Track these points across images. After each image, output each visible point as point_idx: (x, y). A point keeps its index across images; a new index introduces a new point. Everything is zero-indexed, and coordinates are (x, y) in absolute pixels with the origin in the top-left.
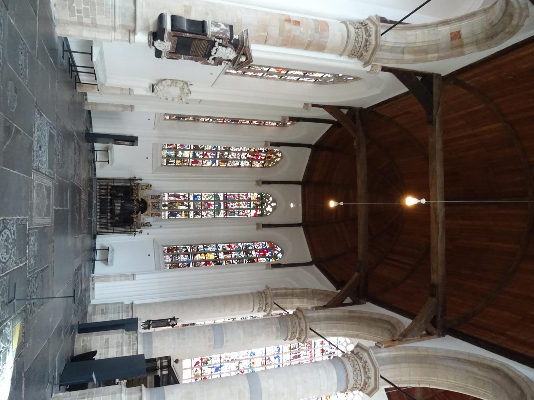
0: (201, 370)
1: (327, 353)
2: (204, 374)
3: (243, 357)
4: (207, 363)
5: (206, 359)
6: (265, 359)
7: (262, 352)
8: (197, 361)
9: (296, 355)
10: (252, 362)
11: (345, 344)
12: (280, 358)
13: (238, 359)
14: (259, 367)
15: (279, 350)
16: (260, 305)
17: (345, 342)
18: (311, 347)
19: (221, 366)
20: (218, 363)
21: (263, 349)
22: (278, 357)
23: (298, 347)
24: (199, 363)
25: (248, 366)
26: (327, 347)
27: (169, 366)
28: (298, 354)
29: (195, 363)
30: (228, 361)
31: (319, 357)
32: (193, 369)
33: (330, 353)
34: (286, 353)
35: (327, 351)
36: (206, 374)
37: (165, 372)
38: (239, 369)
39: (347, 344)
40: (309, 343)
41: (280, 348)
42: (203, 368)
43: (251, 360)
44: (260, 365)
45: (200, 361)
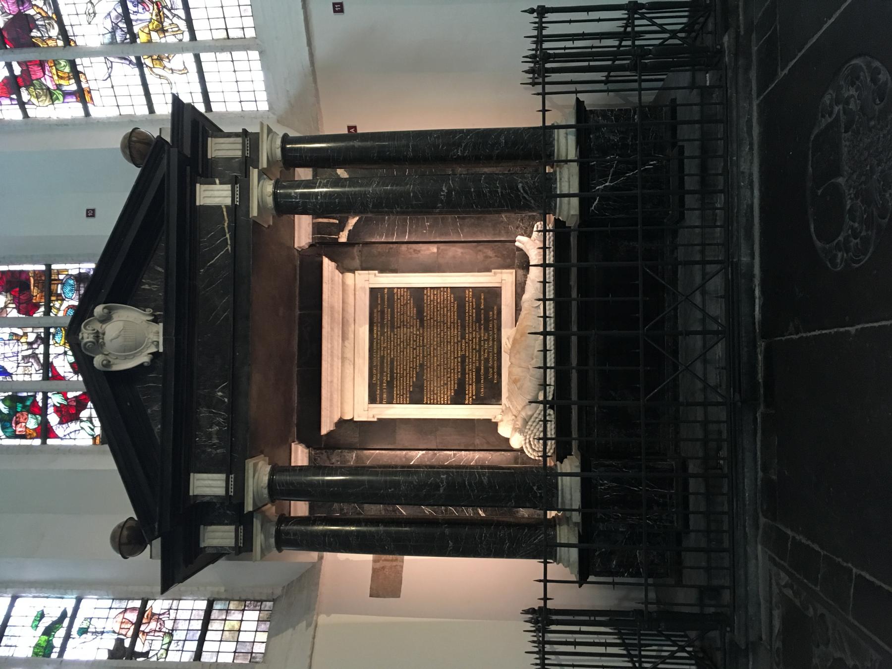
2: (32, 337)
4: (13, 400)
5: (19, 429)
8: (74, 426)
24: (58, 410)
36: (19, 332)
42: (37, 377)
45: (53, 419)
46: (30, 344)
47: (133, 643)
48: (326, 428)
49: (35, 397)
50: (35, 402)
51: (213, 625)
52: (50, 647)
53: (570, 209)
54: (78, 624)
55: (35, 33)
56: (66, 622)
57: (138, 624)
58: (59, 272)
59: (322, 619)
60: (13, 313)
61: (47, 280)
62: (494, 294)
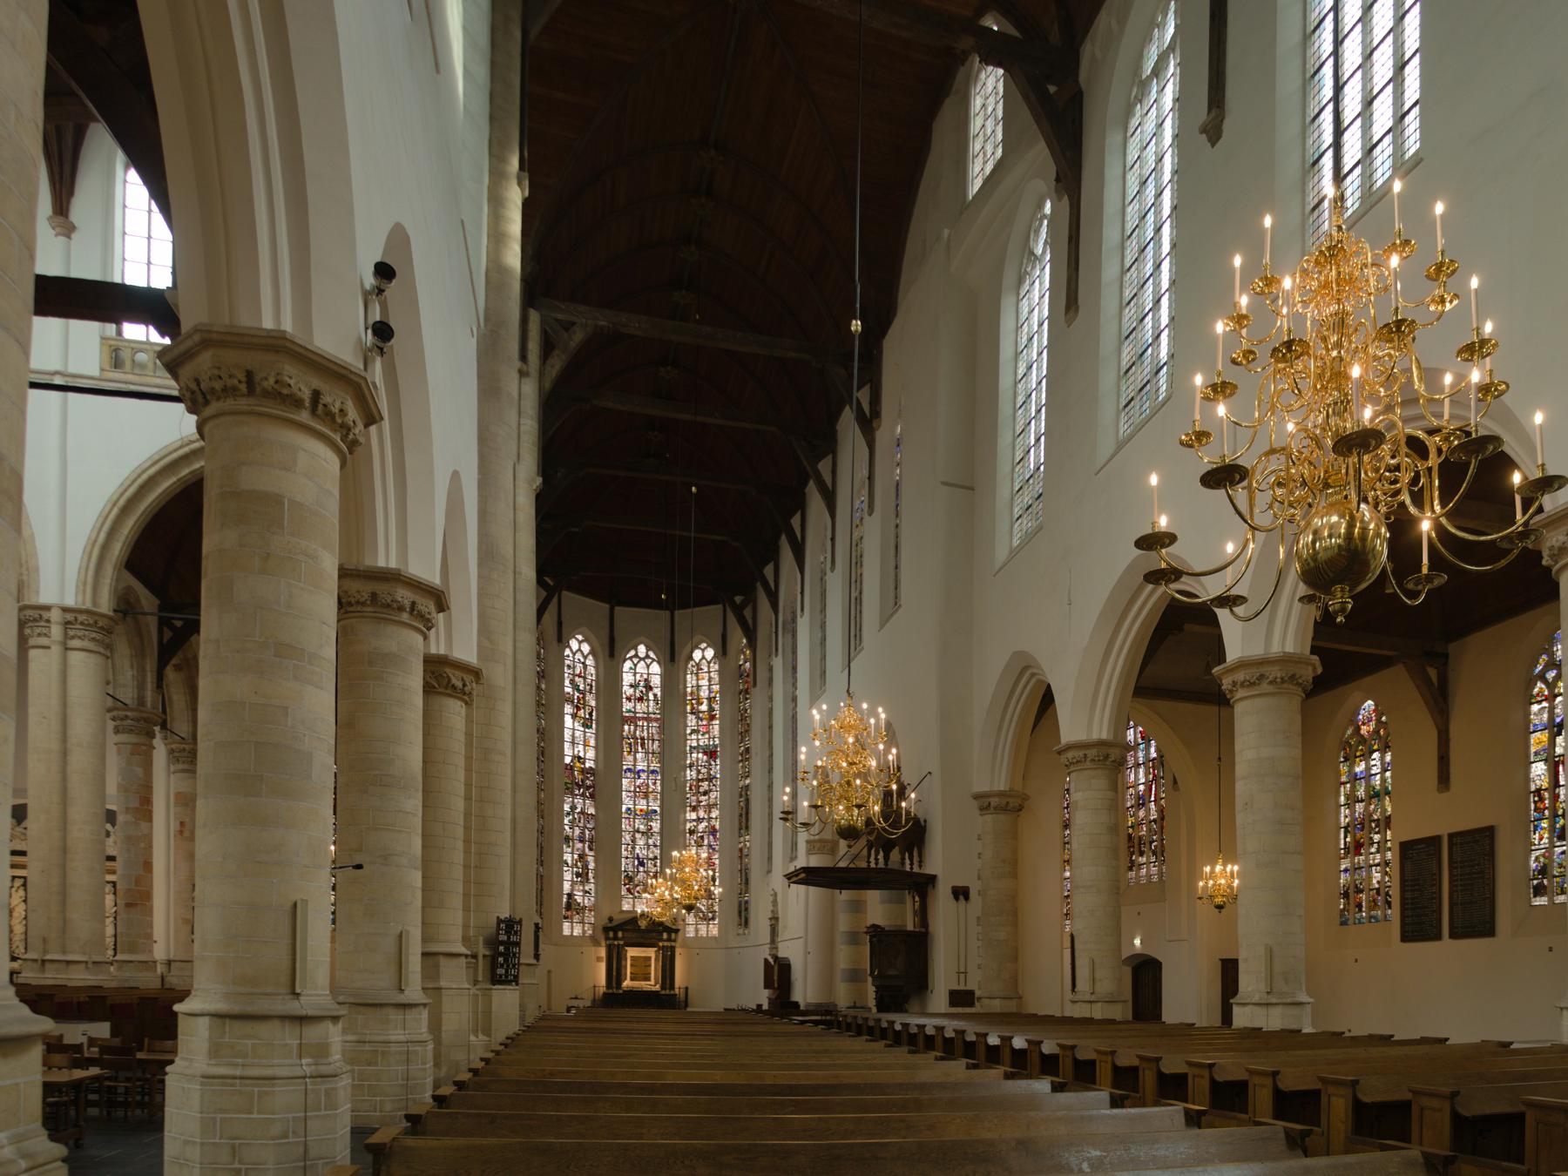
7: (628, 796)
11: (635, 660)
14: (648, 803)
15: (629, 770)
17: (634, 659)
18: (632, 717)
21: (624, 793)
22: (639, 771)
23: (629, 739)
26: (635, 692)
27: (615, 929)
31: (648, 707)
34: (635, 759)
35: (642, 692)
39: (636, 656)
40: (627, 721)
44: (644, 802)
48: (626, 948)
53: (663, 992)
59: (593, 948)
62: (649, 980)
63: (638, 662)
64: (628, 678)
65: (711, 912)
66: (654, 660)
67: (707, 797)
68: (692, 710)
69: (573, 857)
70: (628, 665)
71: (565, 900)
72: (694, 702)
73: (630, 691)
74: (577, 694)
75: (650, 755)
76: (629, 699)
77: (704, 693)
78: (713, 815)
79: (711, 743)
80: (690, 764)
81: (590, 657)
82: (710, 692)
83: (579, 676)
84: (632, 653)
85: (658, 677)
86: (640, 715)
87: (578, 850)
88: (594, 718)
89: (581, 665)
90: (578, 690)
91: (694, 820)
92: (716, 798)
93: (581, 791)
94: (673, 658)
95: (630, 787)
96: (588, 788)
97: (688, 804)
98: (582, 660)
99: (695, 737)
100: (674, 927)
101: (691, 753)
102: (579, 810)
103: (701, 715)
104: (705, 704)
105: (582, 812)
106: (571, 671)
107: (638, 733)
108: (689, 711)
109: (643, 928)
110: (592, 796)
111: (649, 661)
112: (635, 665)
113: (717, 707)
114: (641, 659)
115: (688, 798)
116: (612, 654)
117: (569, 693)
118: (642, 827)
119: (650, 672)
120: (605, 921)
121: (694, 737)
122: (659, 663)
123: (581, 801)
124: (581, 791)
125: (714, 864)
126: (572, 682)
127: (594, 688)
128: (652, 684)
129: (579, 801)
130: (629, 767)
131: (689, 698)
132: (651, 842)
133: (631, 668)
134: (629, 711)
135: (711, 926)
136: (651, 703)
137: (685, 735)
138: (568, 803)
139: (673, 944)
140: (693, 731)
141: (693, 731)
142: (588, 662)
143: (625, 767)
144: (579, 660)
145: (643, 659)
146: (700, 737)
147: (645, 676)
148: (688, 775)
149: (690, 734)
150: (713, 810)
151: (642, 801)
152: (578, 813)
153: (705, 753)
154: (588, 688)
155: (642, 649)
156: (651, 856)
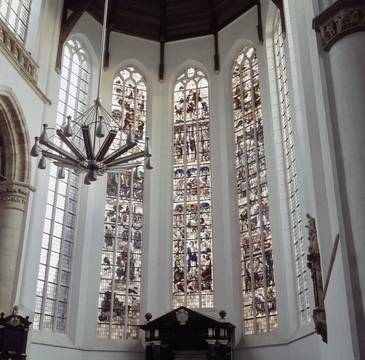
0: (190, 281)
1: (194, 103)
2: (196, 277)
3: (181, 222)
6: (189, 189)
7: (179, 195)
8: (177, 288)
9: (189, 147)
10: (189, 208)
12: (191, 169)
13: (182, 229)
15: (180, 171)
16: (9, 200)
17: (184, 81)
18: (182, 126)
19: (189, 252)
20: (184, 258)
21: (175, 192)
22: (189, 172)
23: (179, 145)
24: (180, 284)
25: (195, 213)
28: (189, 144)
29: (179, 290)
30: (183, 243)
31: (197, 115)
32: (188, 293)
33: (194, 99)
34: (186, 161)
37: (157, 334)
38: (197, 226)
40: (177, 130)
41: (177, 170)
43: (187, 210)
44: (195, 197)
45: (179, 283)
46: (195, 276)
47: (131, 310)
48: (173, 352)
49: (184, 278)
50: (182, 279)
51: (134, 327)
52: (130, 292)
54: (135, 297)
55: (257, 281)
56: (135, 295)
57: (134, 311)
58: (211, 282)
60: (202, 272)
61: (209, 279)
63: (188, 82)
64: (178, 96)
65: (270, 302)
66: (201, 77)
67: (256, 179)
68: (237, 105)
69: (114, 255)
70: (179, 85)
71: (101, 299)
72: (239, 98)
73: (179, 106)
74: (125, 112)
75: (201, 155)
76: (179, 112)
77: (248, 86)
78: (264, 194)
79: (257, 127)
80: (238, 153)
81: (142, 84)
82: (253, 83)
83: (130, 97)
84: (183, 75)
85: (207, 89)
86: (190, 123)
87: (121, 248)
88: (144, 130)
89: (132, 89)
90: (127, 107)
91: (245, 205)
92: (266, 176)
93: (128, 192)
94: (217, 67)
95: (181, 185)
96: (136, 189)
97: (239, 191)
98: (133, 85)
99: (242, 128)
100: (222, 321)
101: (239, 144)
102: (125, 209)
103: (246, 106)
104: (249, 95)
105: (127, 212)
106: (121, 94)
107: (188, 138)
108: (235, 107)
109: (183, 323)
110: (140, 197)
111: (197, 79)
112: (185, 85)
113: (258, 93)
114: (189, 79)
115: (239, 186)
116: (161, 76)
117: (118, 111)
118: (193, 222)
119: (199, 87)
120: (144, 322)
121: (240, 128)
122: (206, 77)
123: (127, 202)
124: (128, 192)
125: (270, 245)
126: (120, 102)
127: (145, 107)
128: (201, 96)
129: (125, 204)
130: (180, 168)
131: (234, 97)
132: (203, 235)
133: (181, 88)
134: (181, 121)
135: (272, 318)
136: (201, 111)
137: (233, 128)
138: (111, 204)
139: (224, 342)
140: (240, 123)
141: (240, 123)
142: (139, 87)
143: (175, 169)
144: (130, 85)
145: (193, 78)
146: (247, 125)
147: (194, 91)
148: (238, 164)
149: (237, 127)
150: (263, 189)
151: (192, 197)
152: (123, 213)
153: (252, 137)
154: (138, 107)
155: (191, 72)
156: (204, 249)
